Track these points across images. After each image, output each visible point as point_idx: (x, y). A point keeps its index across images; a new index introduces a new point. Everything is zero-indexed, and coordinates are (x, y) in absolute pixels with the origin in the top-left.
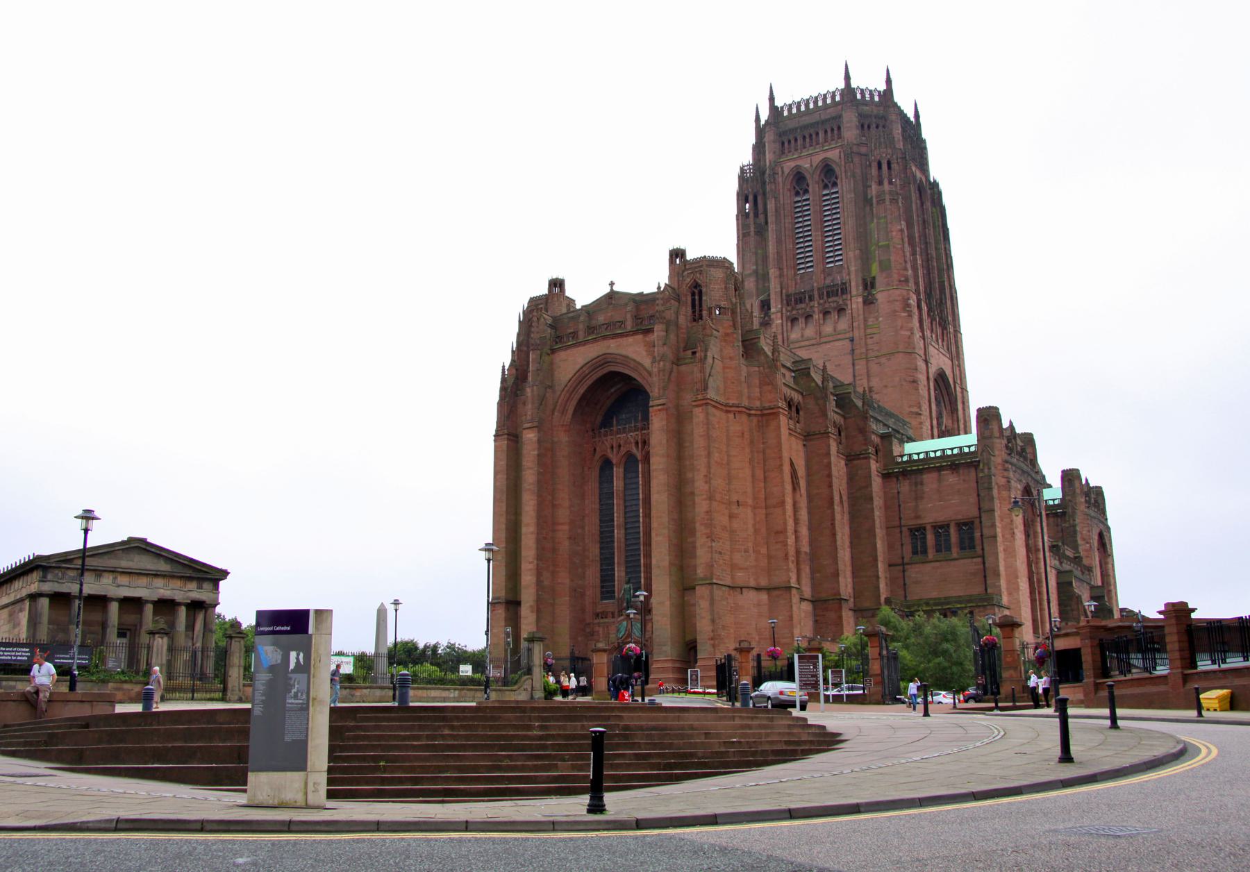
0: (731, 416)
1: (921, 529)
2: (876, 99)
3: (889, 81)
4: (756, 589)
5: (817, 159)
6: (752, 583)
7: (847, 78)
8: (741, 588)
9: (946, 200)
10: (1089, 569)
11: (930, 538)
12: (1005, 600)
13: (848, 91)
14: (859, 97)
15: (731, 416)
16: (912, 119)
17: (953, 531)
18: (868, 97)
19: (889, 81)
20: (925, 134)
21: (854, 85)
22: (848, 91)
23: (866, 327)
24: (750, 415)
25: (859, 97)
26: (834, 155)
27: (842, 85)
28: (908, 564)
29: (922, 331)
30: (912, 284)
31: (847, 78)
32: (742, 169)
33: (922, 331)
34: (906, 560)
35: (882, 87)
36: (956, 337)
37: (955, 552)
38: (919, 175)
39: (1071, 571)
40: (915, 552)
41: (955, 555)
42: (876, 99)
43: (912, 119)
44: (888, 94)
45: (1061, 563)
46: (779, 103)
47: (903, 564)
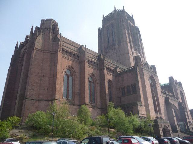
0: (45, 53)
1: (124, 88)
3: (123, 8)
4: (47, 101)
6: (45, 99)
7: (115, 8)
8: (41, 100)
9: (140, 30)
10: (178, 99)
11: (126, 90)
12: (143, 103)
13: (115, 11)
15: (45, 53)
16: (131, 16)
17: (131, 87)
18: (119, 11)
19: (123, 8)
20: (134, 18)
21: (116, 9)
22: (115, 11)
23: (119, 50)
24: (51, 53)
27: (114, 10)
28: (121, 97)
29: (132, 50)
30: (128, 41)
31: (115, 8)
33: (132, 50)
34: (121, 96)
35: (122, 9)
37: (131, 92)
38: (132, 24)
39: (168, 98)
40: (123, 94)
41: (132, 94)
43: (131, 16)
44: (123, 10)
45: (166, 96)
46: (104, 16)
47: (120, 97)
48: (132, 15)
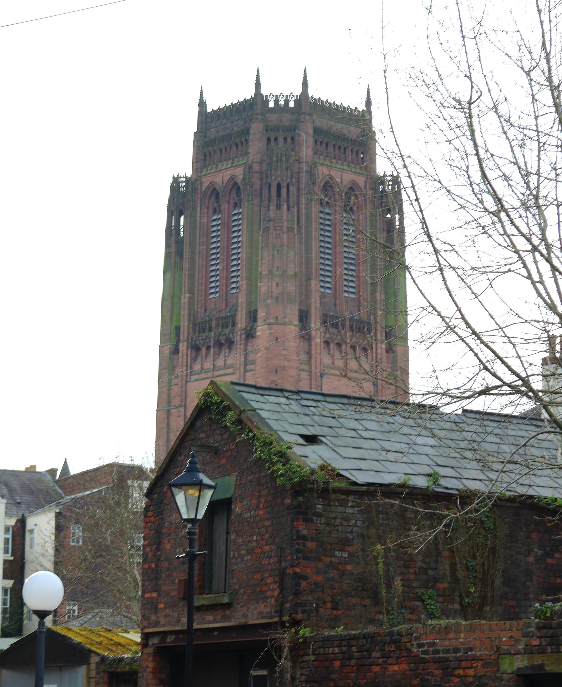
2: (292, 104)
3: (305, 84)
5: (227, 175)
7: (258, 85)
14: (271, 105)
19: (305, 84)
25: (271, 105)
26: (239, 173)
31: (258, 85)
32: (176, 180)
36: (390, 349)
42: (292, 104)
48: (368, 103)
